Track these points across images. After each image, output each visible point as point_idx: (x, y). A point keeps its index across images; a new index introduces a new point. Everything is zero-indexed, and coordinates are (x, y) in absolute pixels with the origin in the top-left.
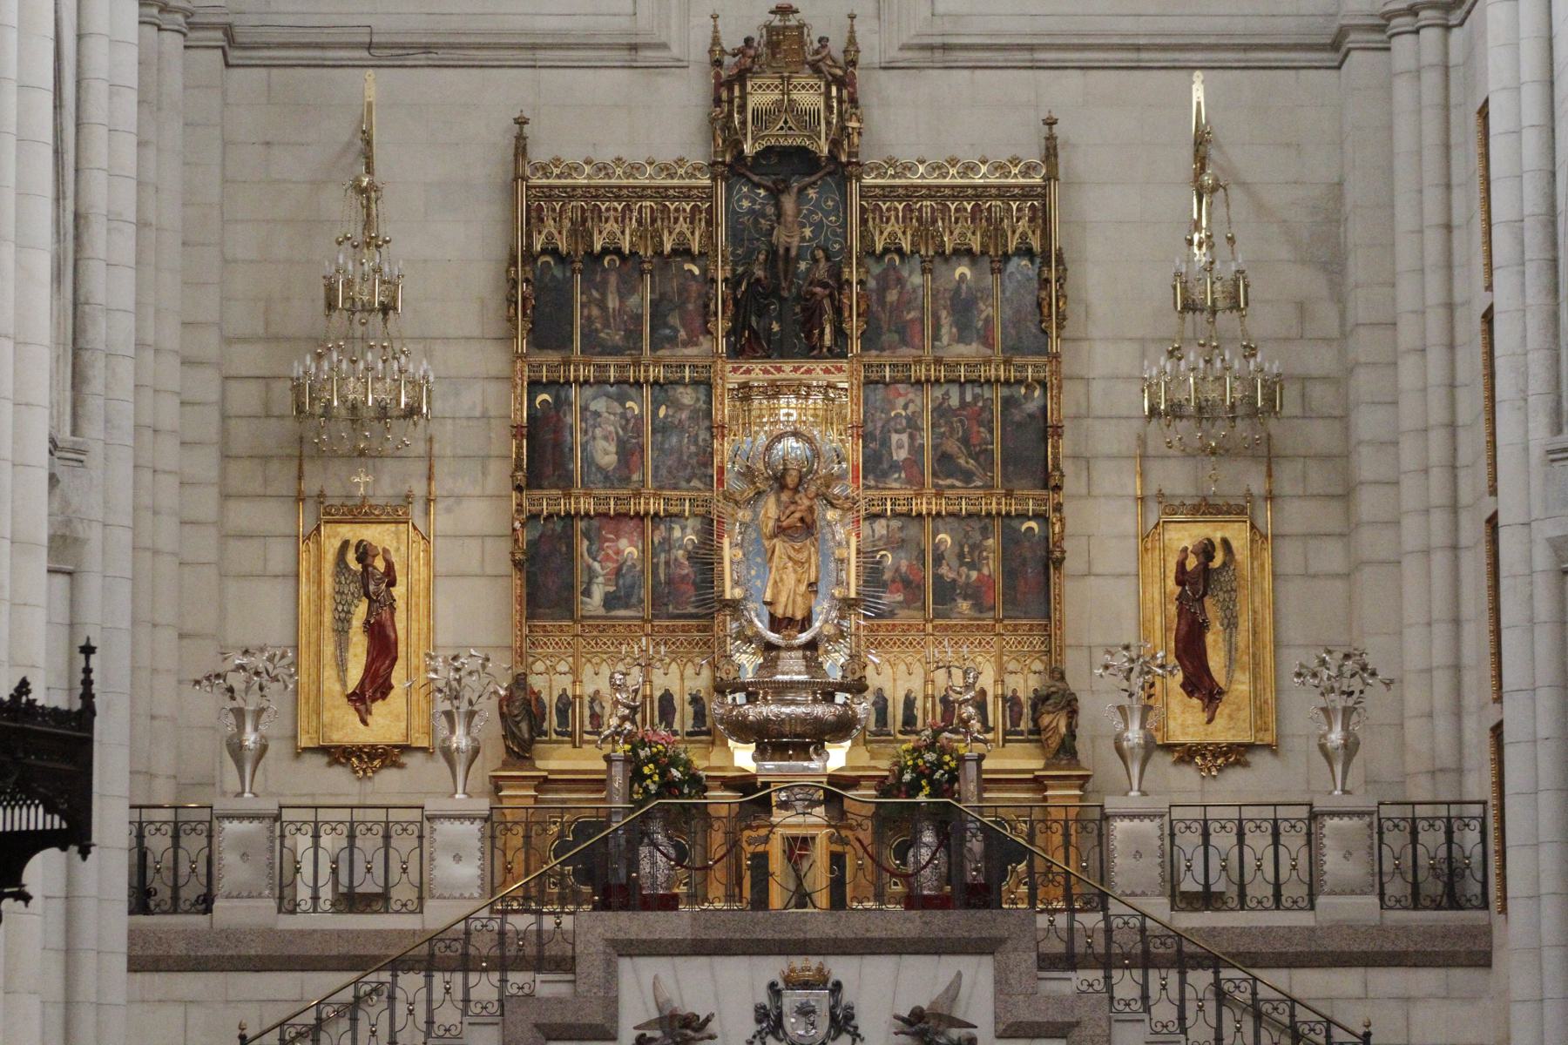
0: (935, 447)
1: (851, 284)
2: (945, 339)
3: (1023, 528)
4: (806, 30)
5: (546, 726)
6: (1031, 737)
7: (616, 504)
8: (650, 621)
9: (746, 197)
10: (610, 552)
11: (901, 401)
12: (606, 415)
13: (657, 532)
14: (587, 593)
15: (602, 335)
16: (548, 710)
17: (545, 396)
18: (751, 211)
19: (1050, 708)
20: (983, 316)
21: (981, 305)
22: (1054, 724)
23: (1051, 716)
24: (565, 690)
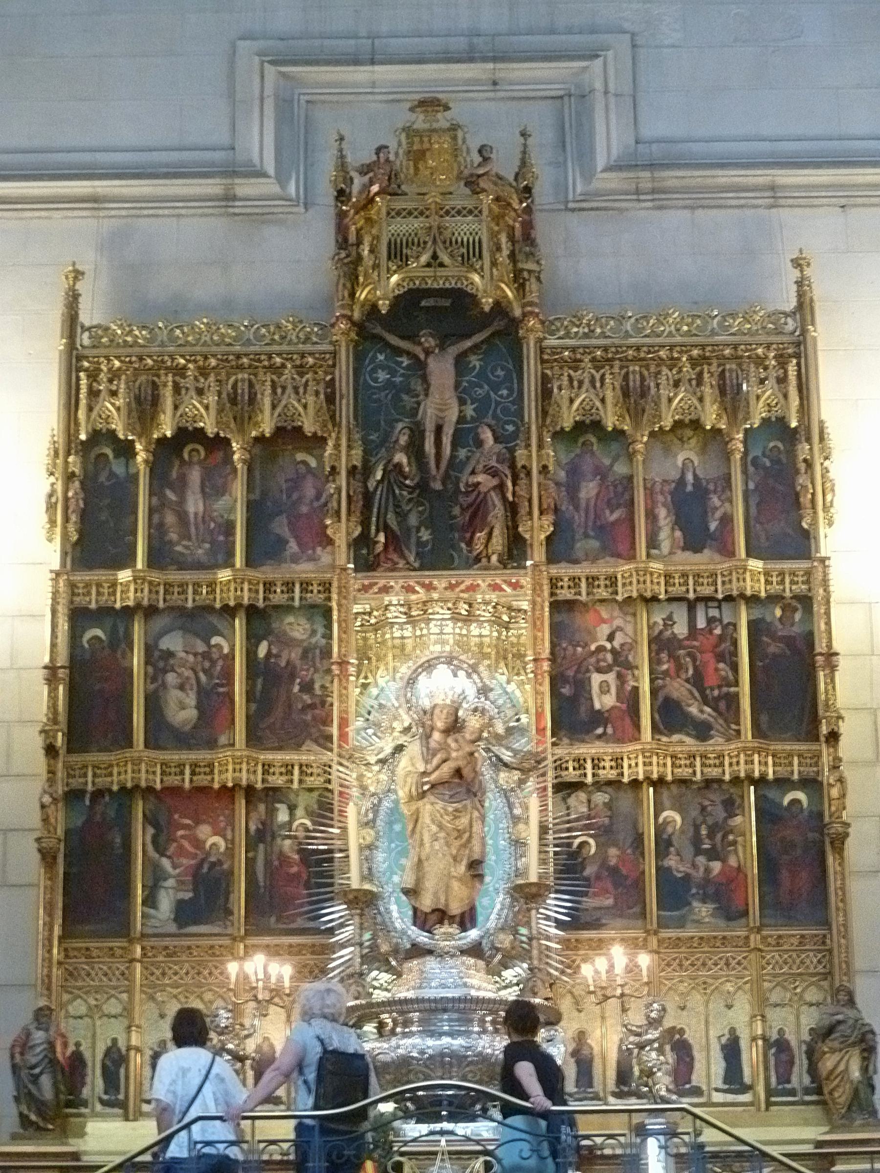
0: (654, 692)
1: (529, 474)
2: (665, 547)
3: (786, 801)
4: (460, 134)
5: (86, 1092)
6: (808, 1098)
7: (193, 773)
8: (242, 939)
9: (383, 368)
10: (186, 844)
11: (604, 630)
12: (183, 655)
13: (254, 816)
14: (150, 901)
15: (179, 548)
16: (89, 1071)
17: (99, 632)
18: (389, 384)
19: (836, 1045)
20: (718, 514)
21: (715, 500)
22: (842, 1067)
23: (836, 1057)
24: (115, 1041)
